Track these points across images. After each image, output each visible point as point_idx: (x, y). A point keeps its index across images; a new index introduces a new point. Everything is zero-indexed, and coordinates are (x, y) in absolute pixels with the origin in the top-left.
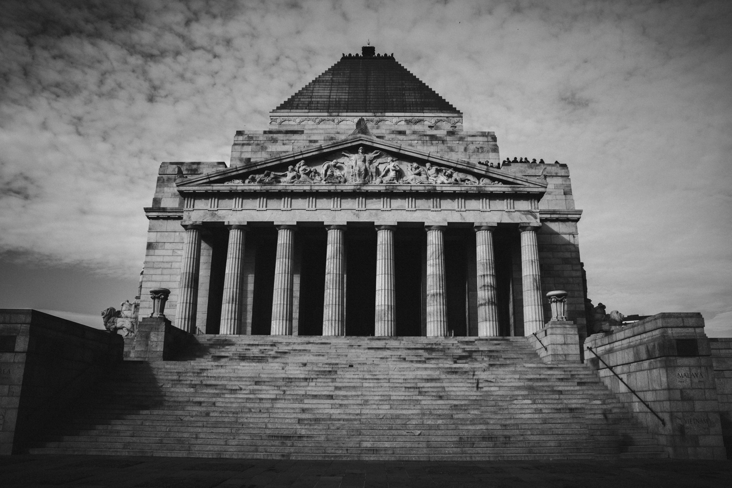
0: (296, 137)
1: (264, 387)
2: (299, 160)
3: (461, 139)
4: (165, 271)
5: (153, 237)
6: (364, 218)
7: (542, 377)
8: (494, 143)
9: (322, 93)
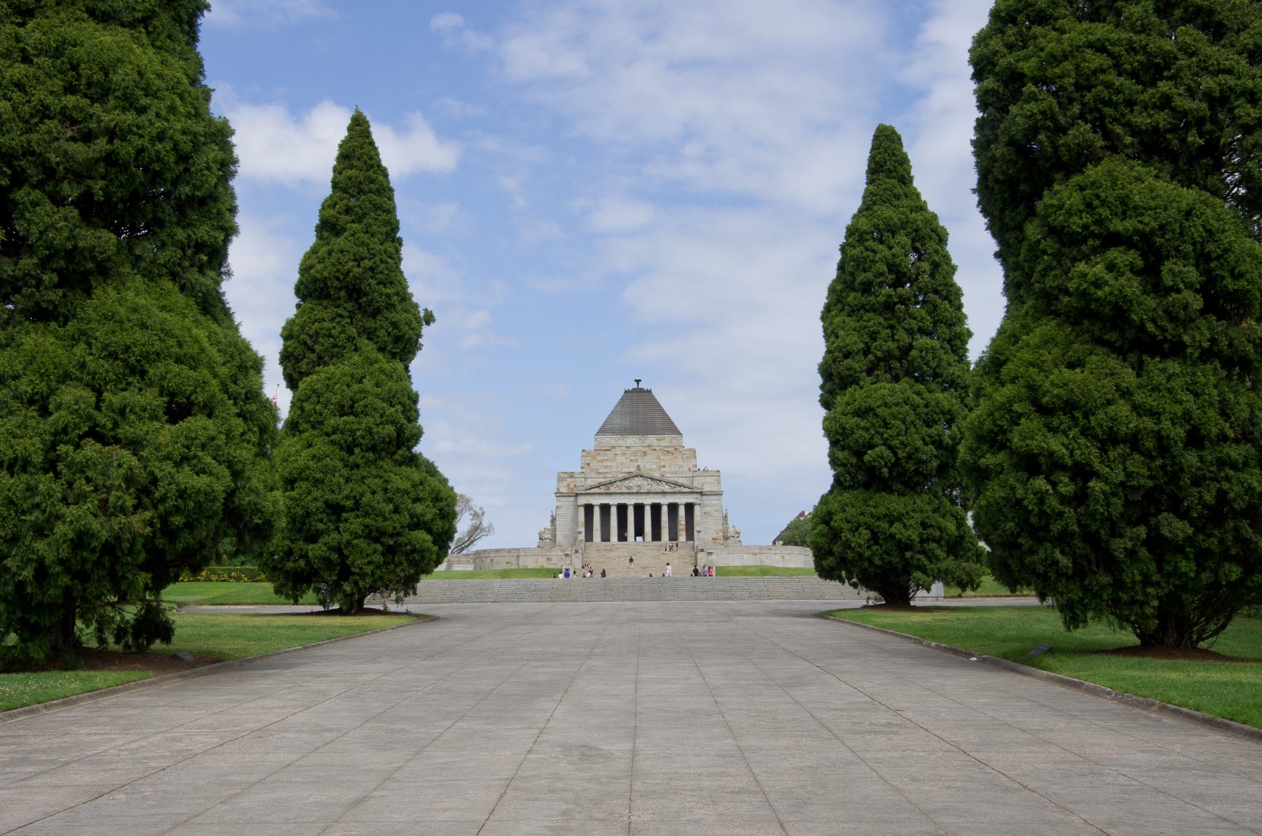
5: (558, 504)
6: (640, 501)
9: (617, 420)
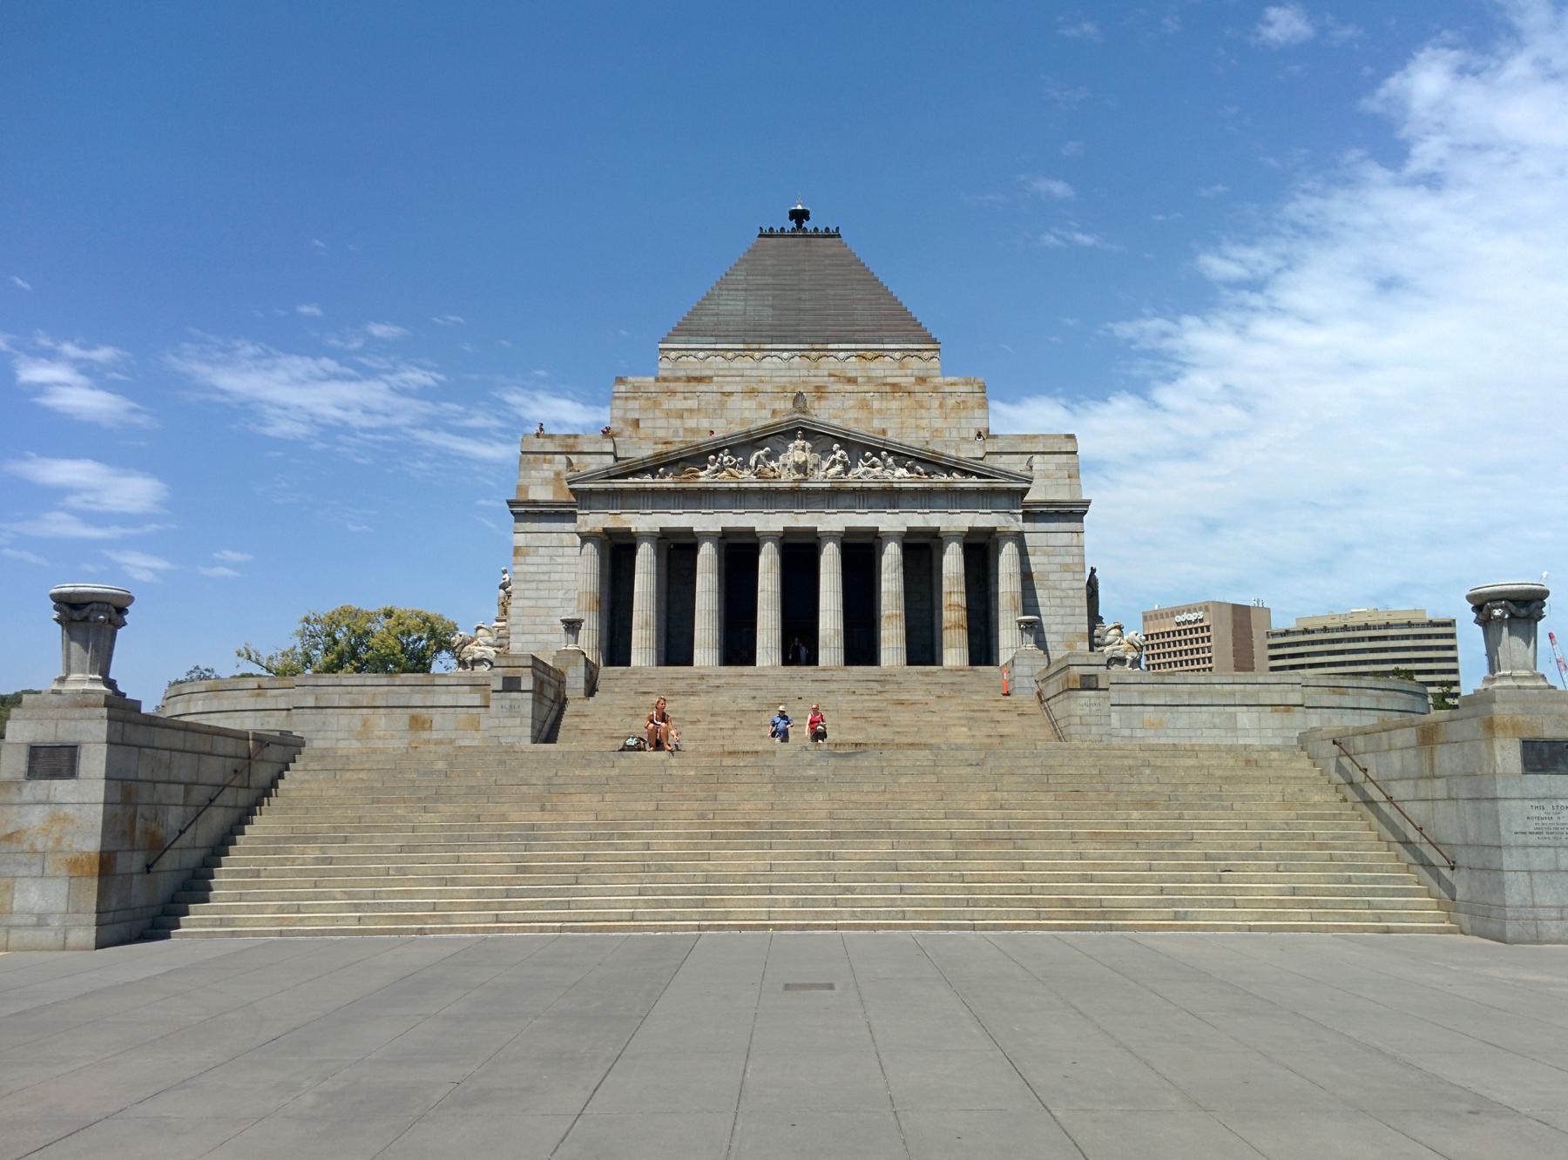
0: (702, 387)
1: (720, 719)
2: (721, 450)
3: (936, 390)
4: (541, 585)
7: (986, 709)
8: (982, 395)
9: (734, 306)
